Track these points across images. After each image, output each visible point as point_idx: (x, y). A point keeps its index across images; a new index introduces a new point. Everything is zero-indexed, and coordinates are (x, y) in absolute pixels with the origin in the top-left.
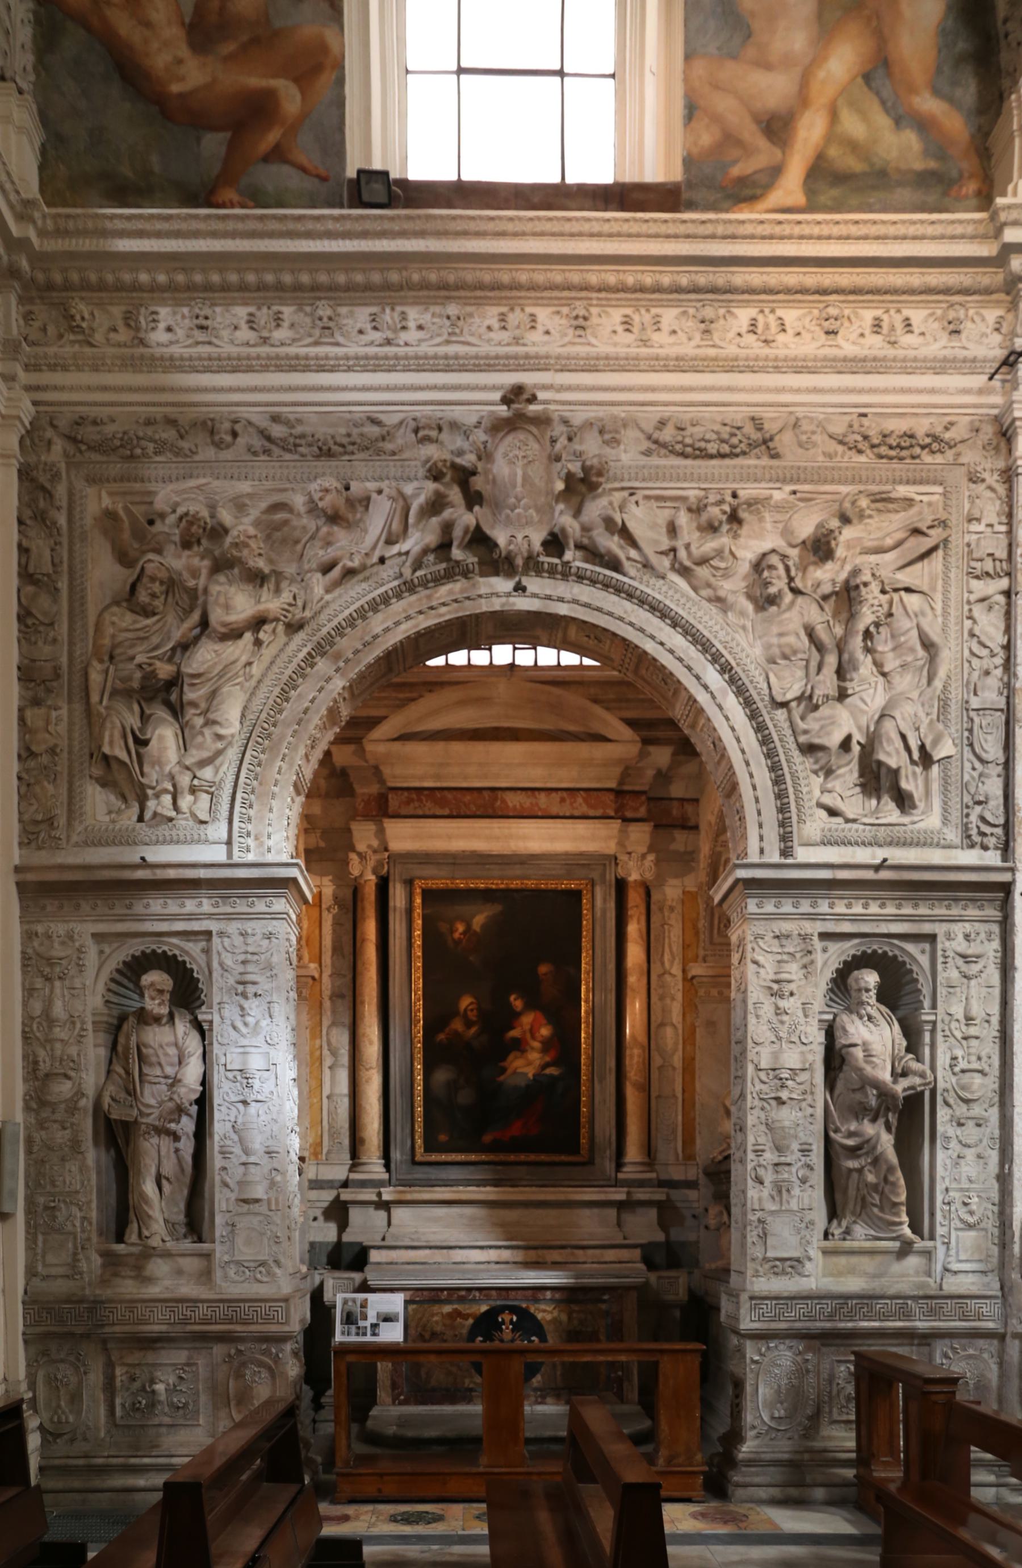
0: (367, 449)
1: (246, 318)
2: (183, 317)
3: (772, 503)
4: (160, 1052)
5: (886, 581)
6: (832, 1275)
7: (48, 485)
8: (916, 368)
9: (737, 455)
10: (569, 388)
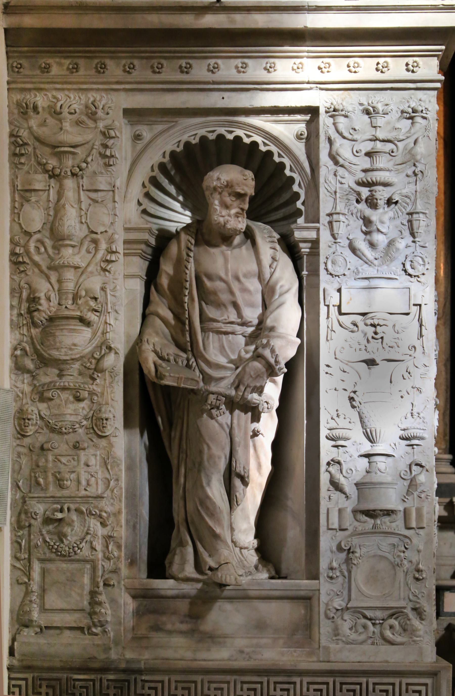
4: (235, 287)
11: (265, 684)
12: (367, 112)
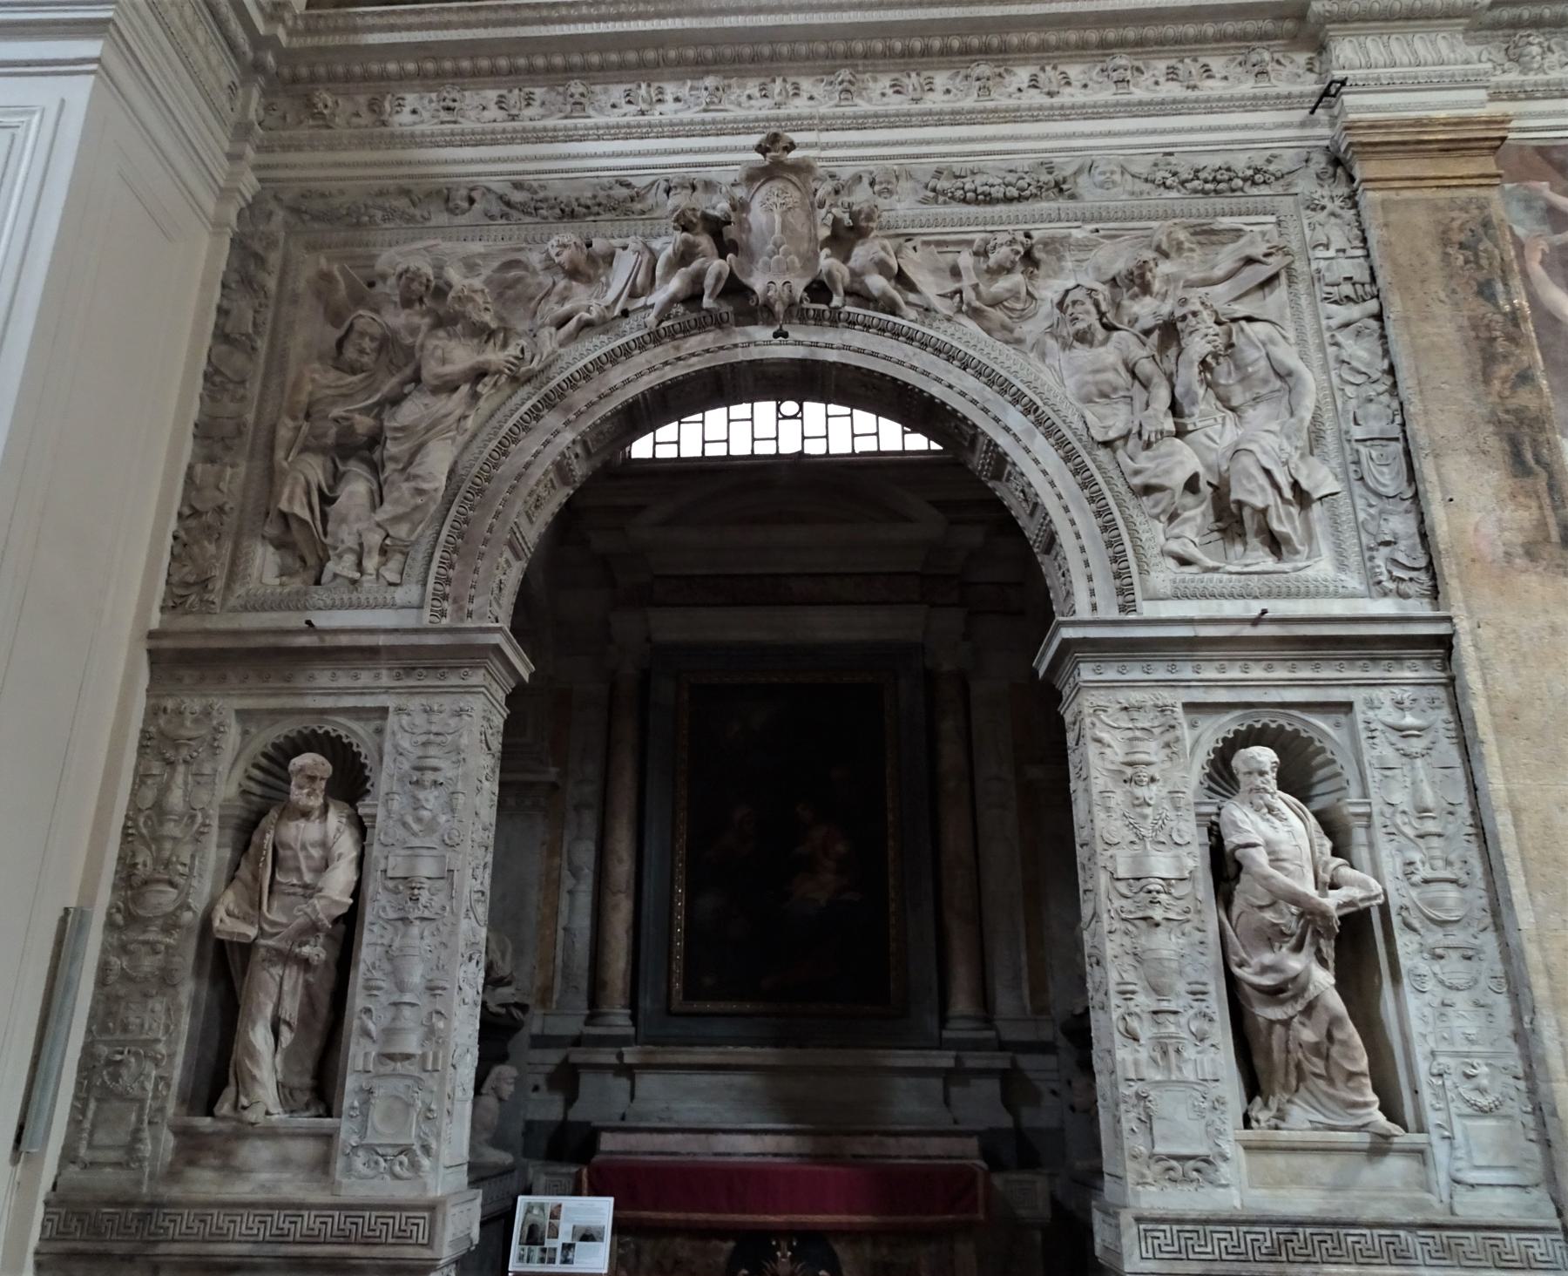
0: (614, 209)
1: (495, 99)
2: (431, 101)
3: (1071, 240)
5: (1220, 312)
6: (1265, 1185)
7: (261, 251)
8: (1223, 107)
9: (1027, 199)
10: (835, 146)
11: (276, 1217)
12: (425, 711)
